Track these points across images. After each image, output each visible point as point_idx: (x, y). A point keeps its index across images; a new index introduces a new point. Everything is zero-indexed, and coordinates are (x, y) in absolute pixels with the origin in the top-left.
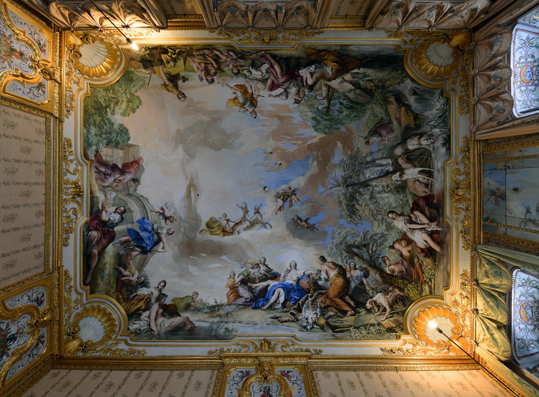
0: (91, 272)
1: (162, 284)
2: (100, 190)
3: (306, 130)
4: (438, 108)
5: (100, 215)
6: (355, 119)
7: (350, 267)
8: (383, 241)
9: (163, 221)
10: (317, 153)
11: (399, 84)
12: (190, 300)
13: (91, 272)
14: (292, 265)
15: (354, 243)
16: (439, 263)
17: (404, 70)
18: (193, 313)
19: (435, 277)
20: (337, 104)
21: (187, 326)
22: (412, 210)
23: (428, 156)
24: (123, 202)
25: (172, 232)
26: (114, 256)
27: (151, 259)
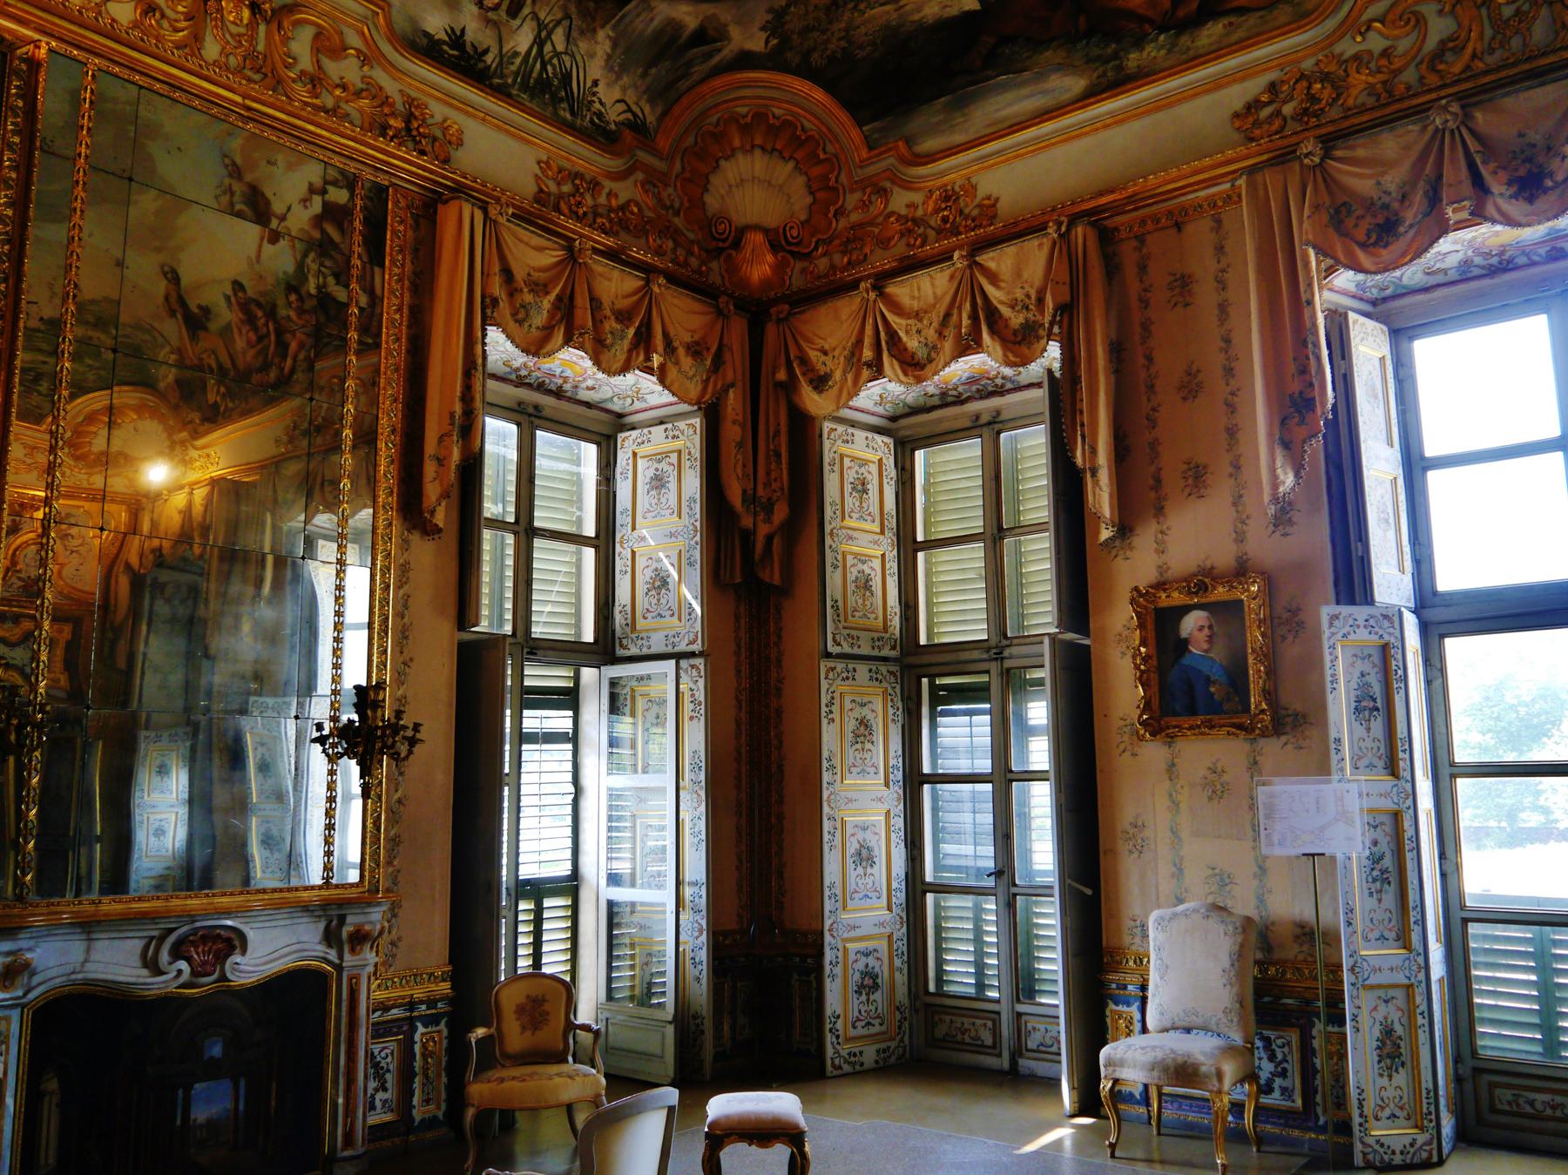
4: (600, 89)
17: (806, 71)
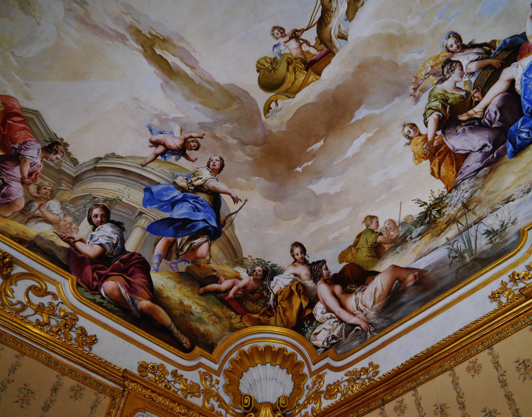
0: (175, 330)
1: (297, 250)
2: (26, 223)
5: (79, 255)
9: (183, 161)
12: (371, 238)
13: (175, 330)
18: (398, 253)
21: (405, 279)
24: (83, 201)
25: (218, 163)
26: (179, 282)
27: (237, 233)
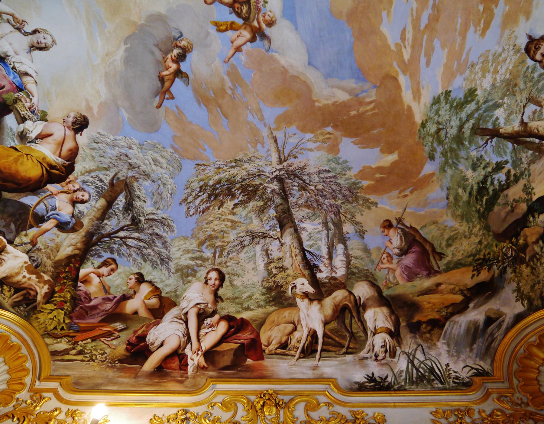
3: (440, 71)
4: (452, 366)
6: (451, 198)
7: (75, 191)
8: (152, 261)
10: (371, 103)
11: (518, 290)
14: (39, 37)
15: (138, 197)
16: (118, 369)
19: (89, 361)
20: (501, 156)
22: (228, 318)
23: (348, 348)
